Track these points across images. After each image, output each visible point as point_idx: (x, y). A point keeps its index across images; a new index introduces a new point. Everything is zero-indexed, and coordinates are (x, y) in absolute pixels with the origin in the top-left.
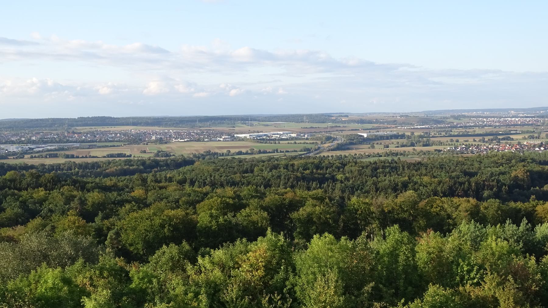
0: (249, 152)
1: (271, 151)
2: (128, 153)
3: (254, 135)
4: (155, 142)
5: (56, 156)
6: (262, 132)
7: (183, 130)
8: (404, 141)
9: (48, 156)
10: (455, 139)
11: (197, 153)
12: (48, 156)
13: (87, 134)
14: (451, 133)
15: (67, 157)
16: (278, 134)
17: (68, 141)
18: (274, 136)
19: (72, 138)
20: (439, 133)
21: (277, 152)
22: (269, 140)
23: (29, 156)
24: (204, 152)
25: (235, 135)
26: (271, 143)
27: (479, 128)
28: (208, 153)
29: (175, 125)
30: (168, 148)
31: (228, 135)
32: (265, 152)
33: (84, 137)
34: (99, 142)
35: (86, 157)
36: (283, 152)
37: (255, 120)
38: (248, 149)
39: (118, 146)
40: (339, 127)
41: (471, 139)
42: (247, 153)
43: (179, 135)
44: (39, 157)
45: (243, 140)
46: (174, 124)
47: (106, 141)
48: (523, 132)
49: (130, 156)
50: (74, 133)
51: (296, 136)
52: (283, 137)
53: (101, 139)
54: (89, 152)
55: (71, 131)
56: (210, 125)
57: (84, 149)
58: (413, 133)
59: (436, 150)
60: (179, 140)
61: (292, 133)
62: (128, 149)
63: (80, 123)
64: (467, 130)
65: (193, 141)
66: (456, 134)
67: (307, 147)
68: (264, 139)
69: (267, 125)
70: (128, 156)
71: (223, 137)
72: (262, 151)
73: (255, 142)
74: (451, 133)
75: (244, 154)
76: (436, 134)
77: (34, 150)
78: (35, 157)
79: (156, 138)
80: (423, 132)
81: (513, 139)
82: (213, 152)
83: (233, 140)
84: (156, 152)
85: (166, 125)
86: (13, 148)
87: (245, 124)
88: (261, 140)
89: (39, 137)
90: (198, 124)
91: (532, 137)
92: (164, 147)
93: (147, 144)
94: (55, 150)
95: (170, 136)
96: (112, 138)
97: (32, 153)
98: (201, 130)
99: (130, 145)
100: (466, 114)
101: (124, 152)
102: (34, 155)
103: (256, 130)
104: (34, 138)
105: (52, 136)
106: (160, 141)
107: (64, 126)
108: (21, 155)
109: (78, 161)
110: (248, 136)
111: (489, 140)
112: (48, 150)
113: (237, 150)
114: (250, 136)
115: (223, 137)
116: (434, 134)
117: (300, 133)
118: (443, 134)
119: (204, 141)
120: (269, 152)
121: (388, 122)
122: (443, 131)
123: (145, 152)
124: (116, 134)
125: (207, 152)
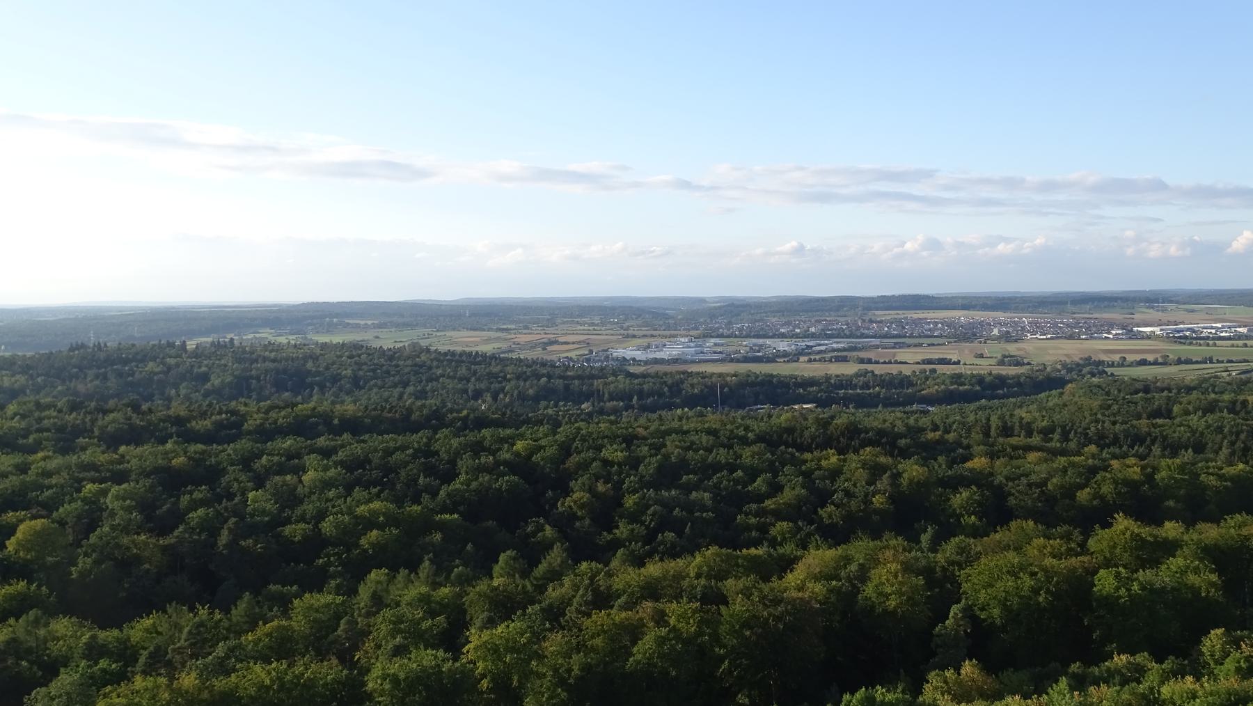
0: (1160, 360)
1: (1199, 360)
2: (955, 359)
3: (1169, 329)
4: (998, 339)
5: (844, 360)
6: (1182, 323)
7: (1045, 318)
9: (833, 360)
11: (1068, 361)
12: (833, 360)
13: (892, 323)
15: (862, 361)
16: (1212, 328)
17: (863, 336)
18: (1205, 331)
19: (868, 329)
21: (1211, 362)
22: (1196, 338)
23: (806, 358)
24: (1081, 359)
25: (1135, 329)
26: (1200, 345)
28: (1088, 361)
29: (1030, 309)
30: (1019, 349)
31: (1122, 329)
32: (1188, 362)
33: (886, 329)
34: (909, 337)
35: (890, 363)
36: (1222, 362)
37: (1171, 302)
38: (1158, 356)
39: (939, 345)
42: (1156, 363)
43: (1037, 328)
44: (820, 360)
45: (1149, 337)
46: (1029, 307)
47: (920, 337)
49: (958, 363)
50: (871, 321)
51: (1246, 331)
52: (1222, 335)
53: (912, 333)
54: (894, 355)
55: (867, 318)
56: (1090, 309)
57: (886, 348)
60: (1038, 336)
61: (1240, 327)
62: (953, 349)
63: (882, 305)
65: (1061, 338)
68: (1186, 337)
69: (1193, 311)
70: (955, 363)
71: (1114, 332)
72: (1183, 359)
73: (1171, 342)
75: (1150, 364)
77: (814, 348)
78: (815, 360)
79: (999, 331)
82: (1097, 360)
83: (1130, 338)
84: (999, 356)
85: (1016, 310)
86: (783, 345)
87: (1153, 308)
88: (1183, 340)
89: (820, 327)
90: (1070, 308)
92: (1012, 348)
93: (985, 343)
94: (844, 350)
95: (1023, 329)
96: (930, 330)
97: (810, 354)
98: (1075, 318)
99: (960, 344)
101: (948, 357)
102: (813, 357)
103: (1172, 319)
104: (813, 330)
105: (839, 326)
106: (1006, 337)
107: (857, 310)
108: (793, 357)
109: (879, 370)
110: (1157, 330)
112: (834, 350)
113: (1138, 357)
114: (1161, 330)
115: (1114, 332)
119: (1079, 338)
120: (1197, 362)
123: (981, 356)
124: (936, 324)
125: (1086, 359)
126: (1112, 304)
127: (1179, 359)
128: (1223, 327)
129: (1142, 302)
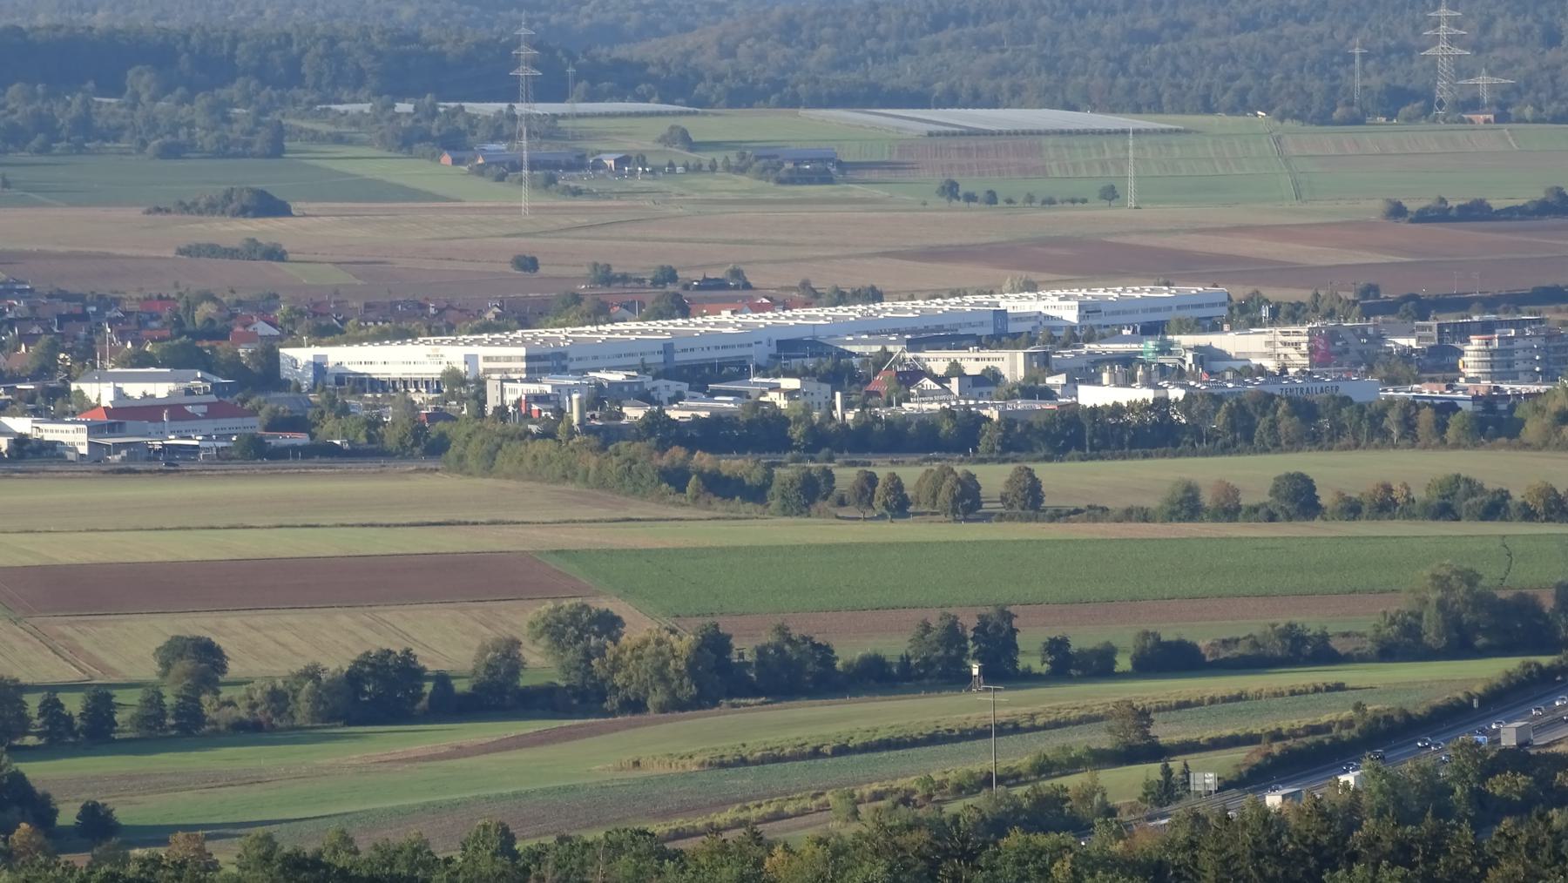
3: (614, 355)
16: (1001, 333)
18: (938, 361)
25: (300, 356)
26: (900, 506)
31: (179, 360)
36: (1099, 666)
51: (1298, 360)
52: (1091, 396)
61: (1245, 316)
67: (1491, 574)
71: (100, 393)
72: (744, 648)
73: (630, 481)
83: (257, 452)
87: (455, 142)
114: (539, 365)
115: (100, 393)
117: (1372, 303)
126: (67, 110)
127: (714, 644)
128: (1096, 323)
129: (356, 83)
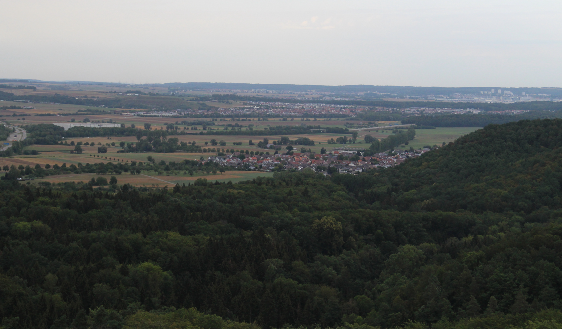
8: (133, 140)
10: (218, 138)
14: (213, 127)
20: (193, 126)
27: (259, 120)
40: (20, 108)
41: (245, 140)
48: (330, 131)
58: (148, 126)
59: (187, 162)
64: (240, 123)
66: (221, 129)
74: (213, 127)
76: (188, 129)
80: (166, 124)
81: (312, 143)
91: (343, 141)
100: (239, 93)
111: (274, 143)
116: (185, 128)
118: (200, 128)
121: (107, 103)
122: (199, 124)
